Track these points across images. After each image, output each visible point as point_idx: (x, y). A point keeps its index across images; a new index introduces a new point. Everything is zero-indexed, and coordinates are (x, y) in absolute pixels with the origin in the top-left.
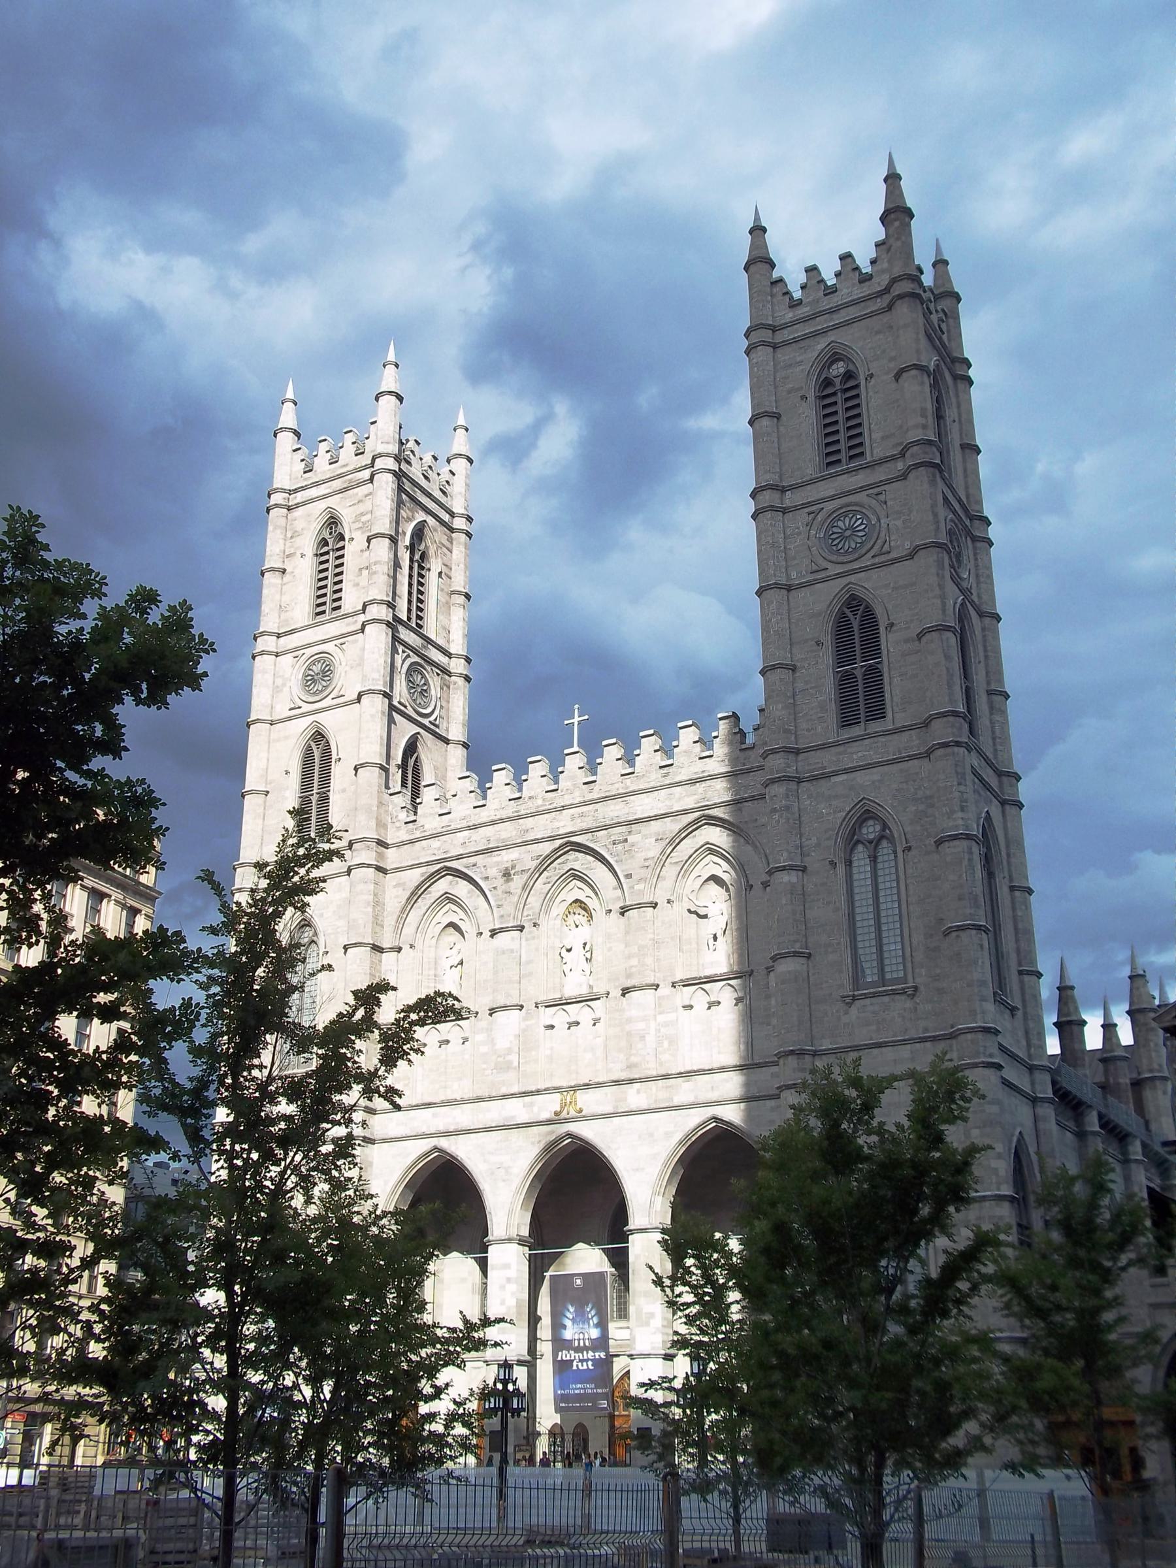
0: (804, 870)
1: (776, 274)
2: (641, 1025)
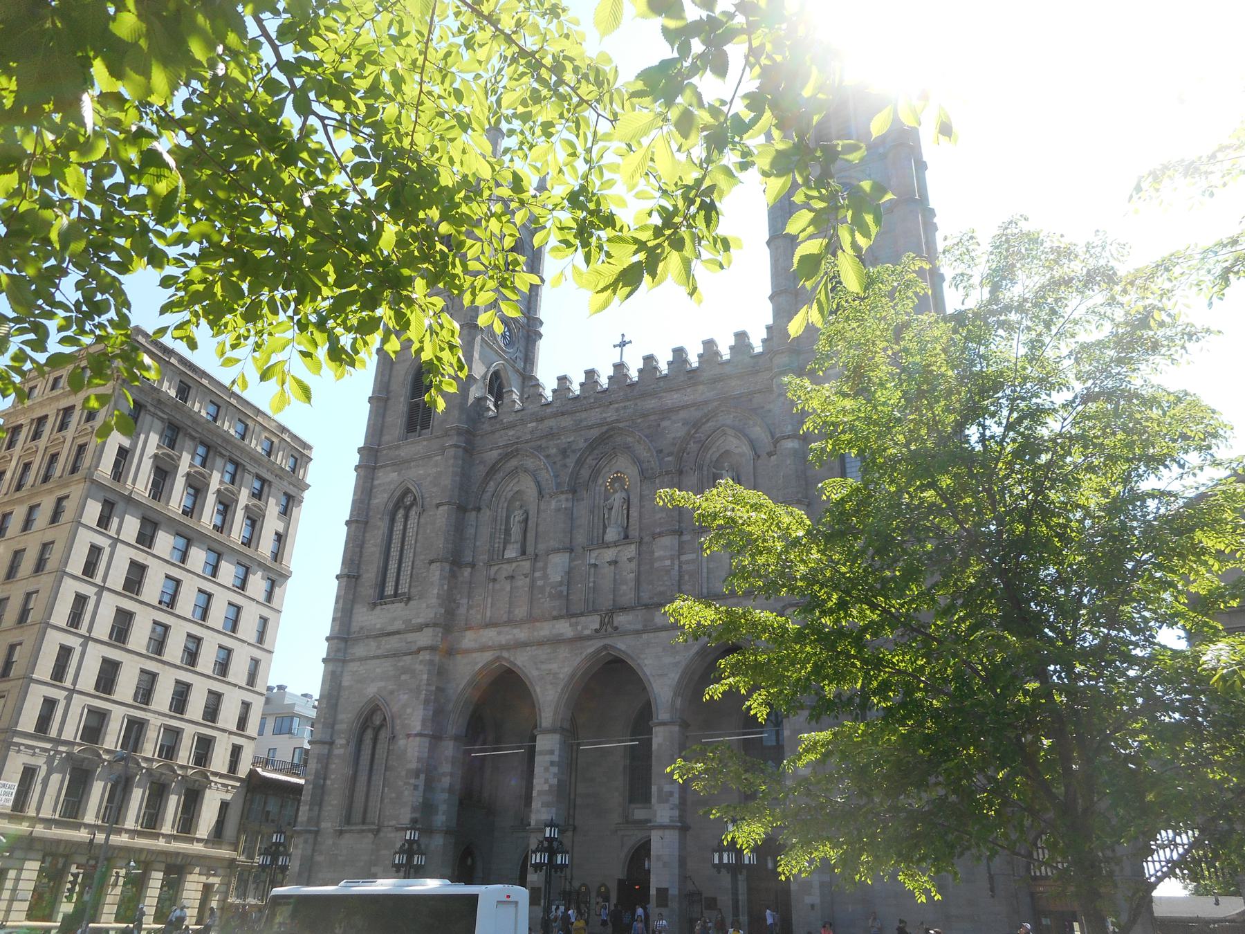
2: (668, 563)
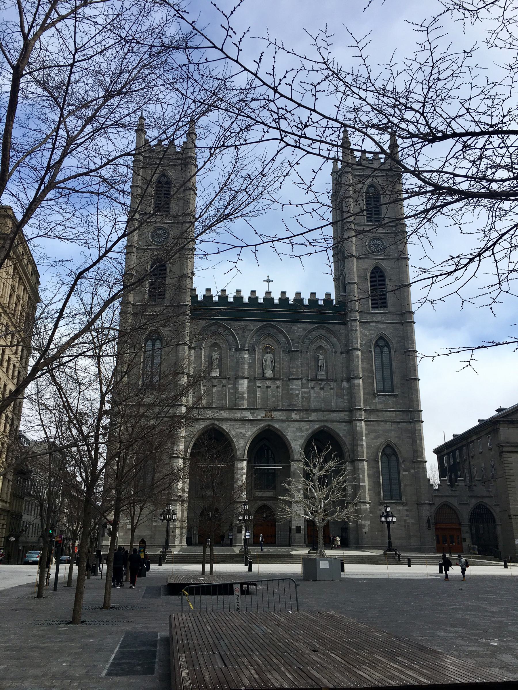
2: (297, 392)
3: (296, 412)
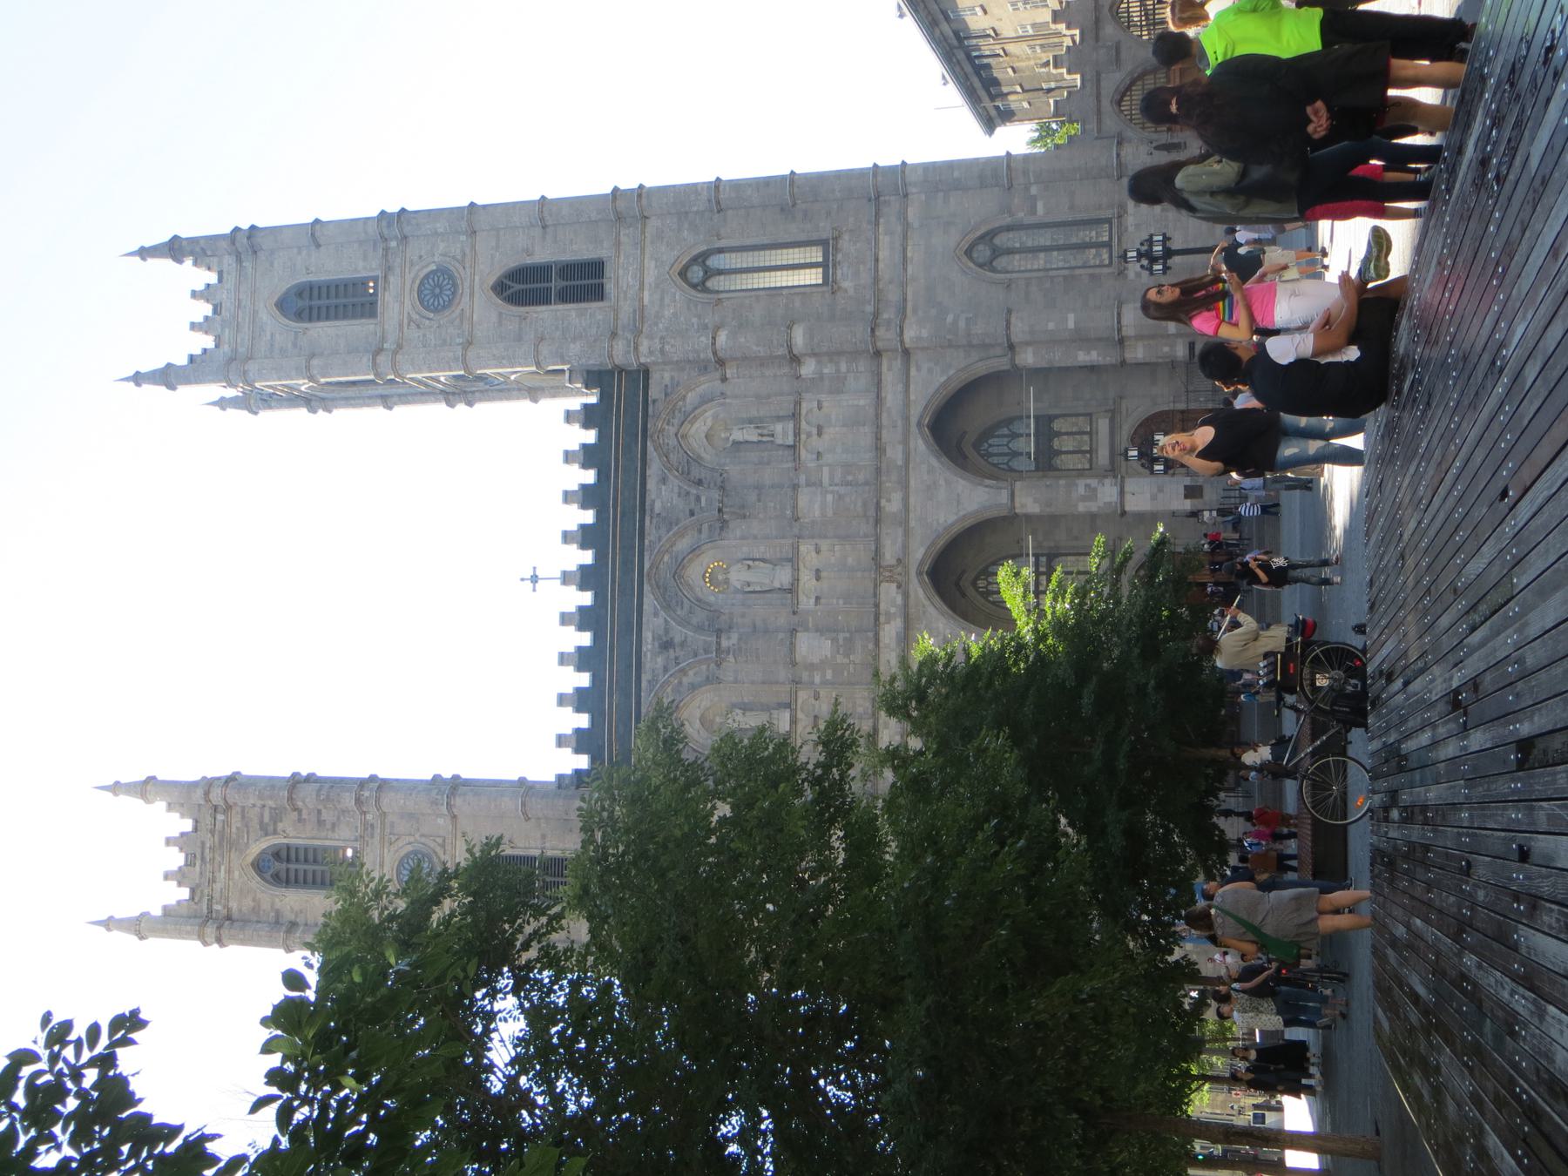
0: (717, 328)
1: (182, 361)
2: (829, 497)
3: (883, 502)
